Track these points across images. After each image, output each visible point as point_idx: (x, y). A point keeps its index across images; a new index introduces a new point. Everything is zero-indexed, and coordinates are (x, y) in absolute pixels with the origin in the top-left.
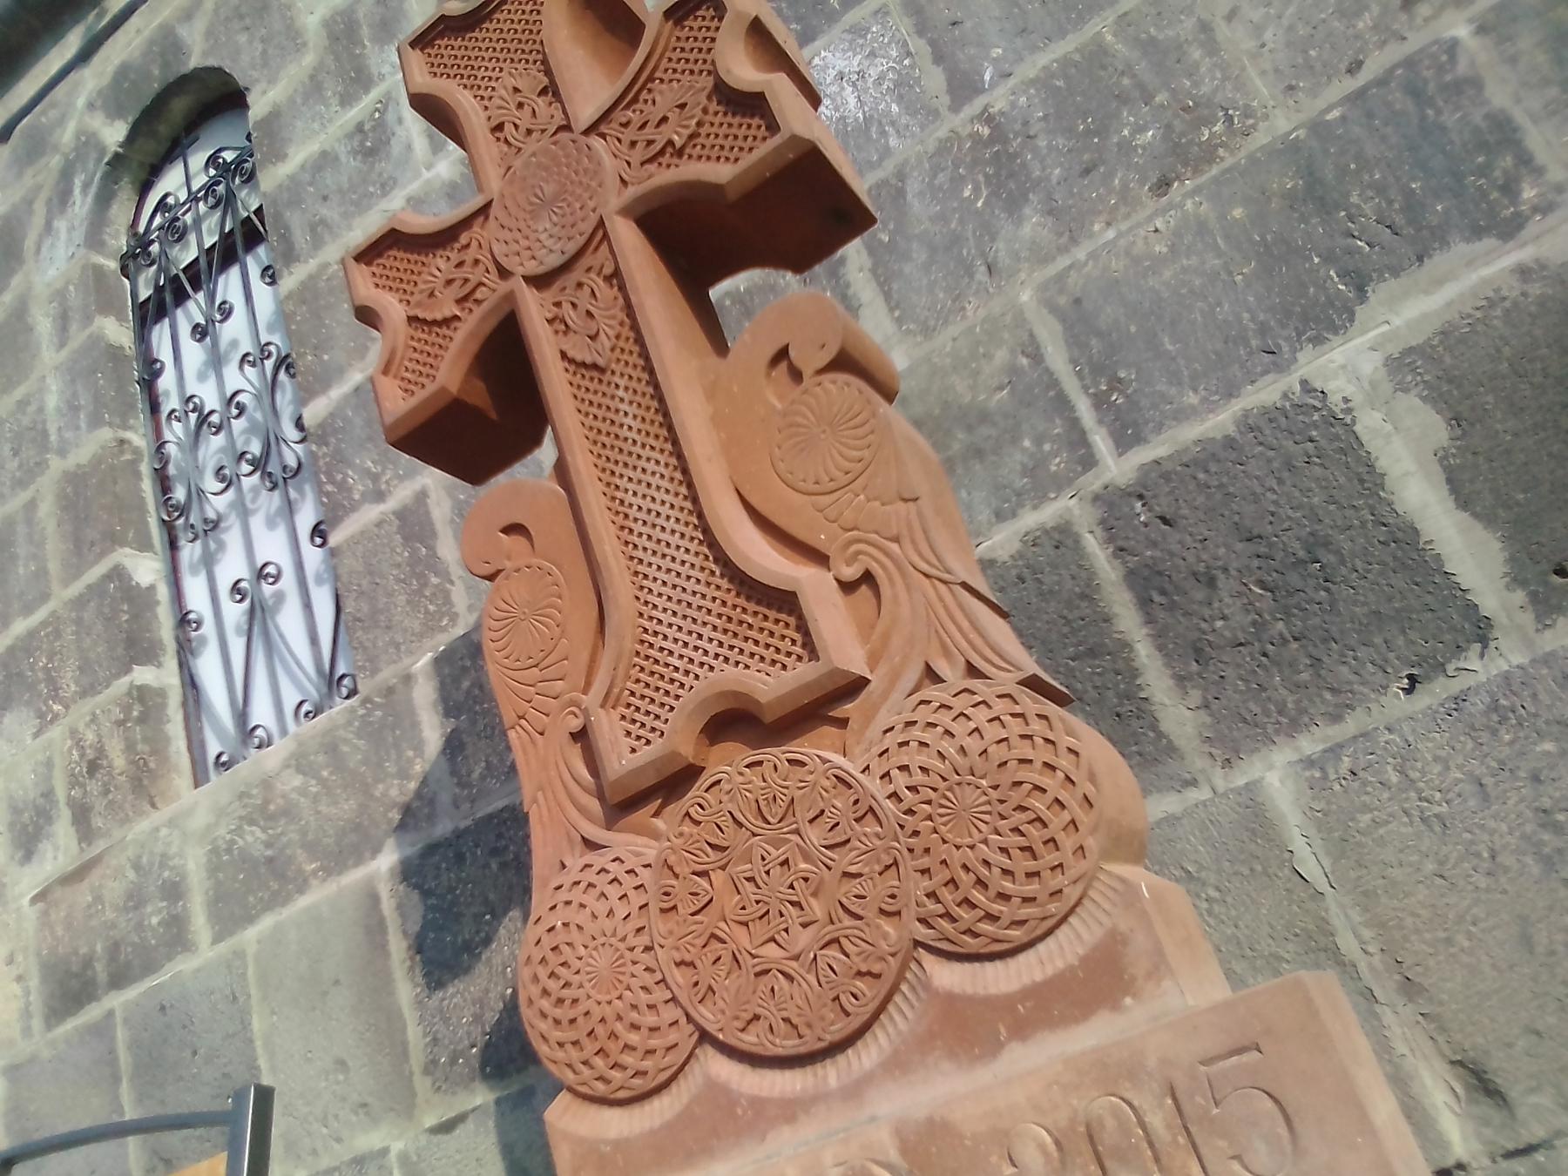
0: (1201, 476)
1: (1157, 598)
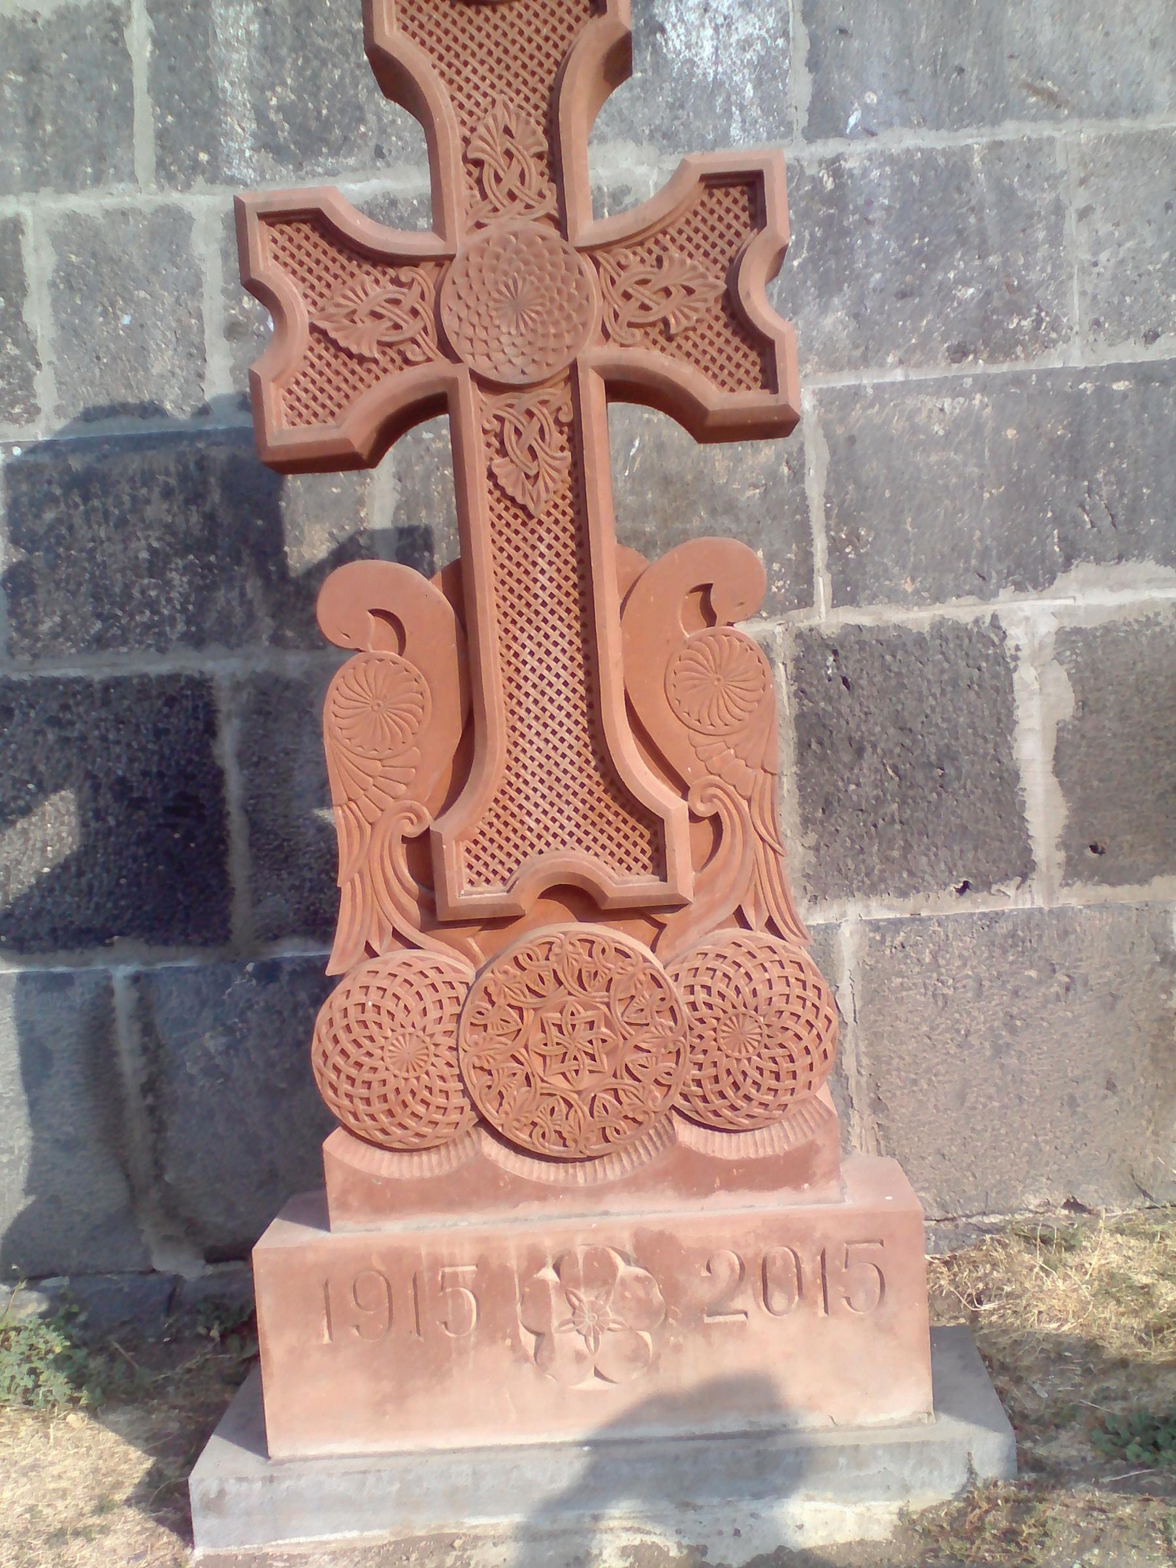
0: (888, 658)
1: (814, 746)
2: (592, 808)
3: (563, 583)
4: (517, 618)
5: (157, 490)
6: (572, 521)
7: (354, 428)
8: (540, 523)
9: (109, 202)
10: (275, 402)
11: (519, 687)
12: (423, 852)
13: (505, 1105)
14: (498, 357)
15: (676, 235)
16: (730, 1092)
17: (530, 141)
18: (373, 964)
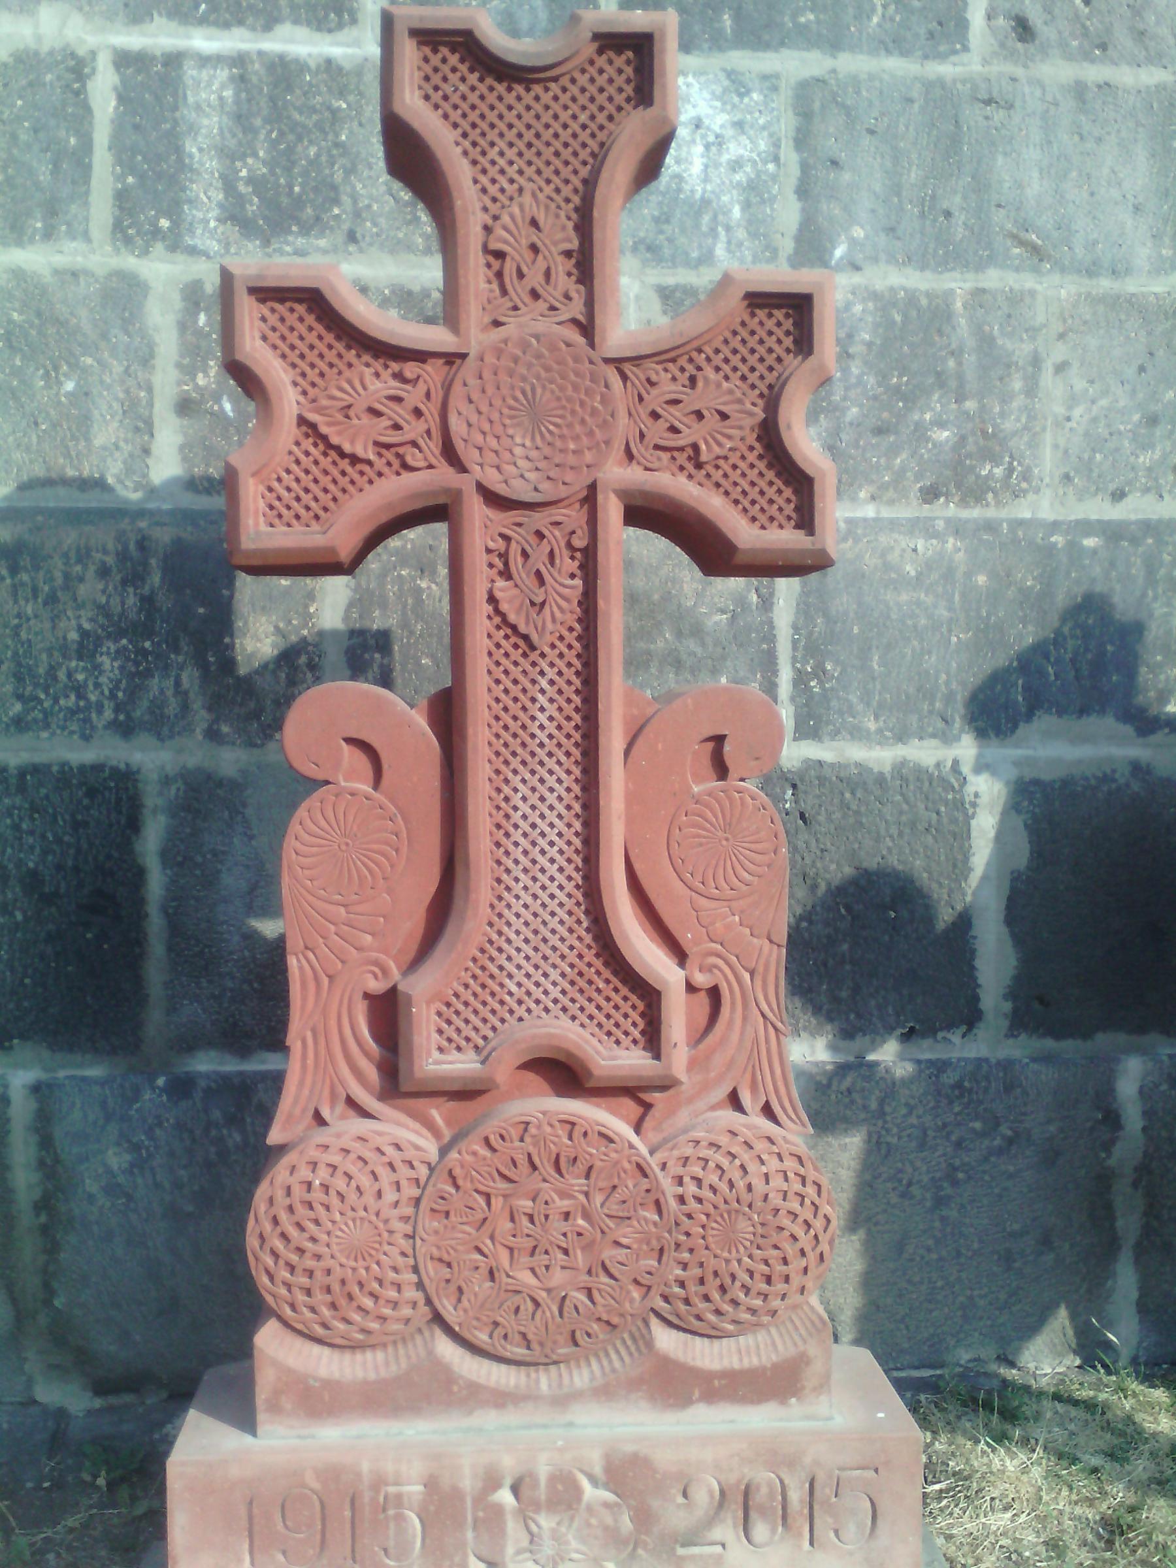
0: (848, 795)
2: (581, 974)
3: (564, 723)
4: (510, 758)
5: (92, 569)
6: (579, 656)
7: (340, 533)
8: (543, 655)
9: (60, 260)
10: (252, 496)
11: (507, 835)
12: (388, 1014)
13: (464, 1299)
14: (510, 469)
15: (712, 355)
16: (716, 1296)
17: (559, 236)
18: (322, 1136)
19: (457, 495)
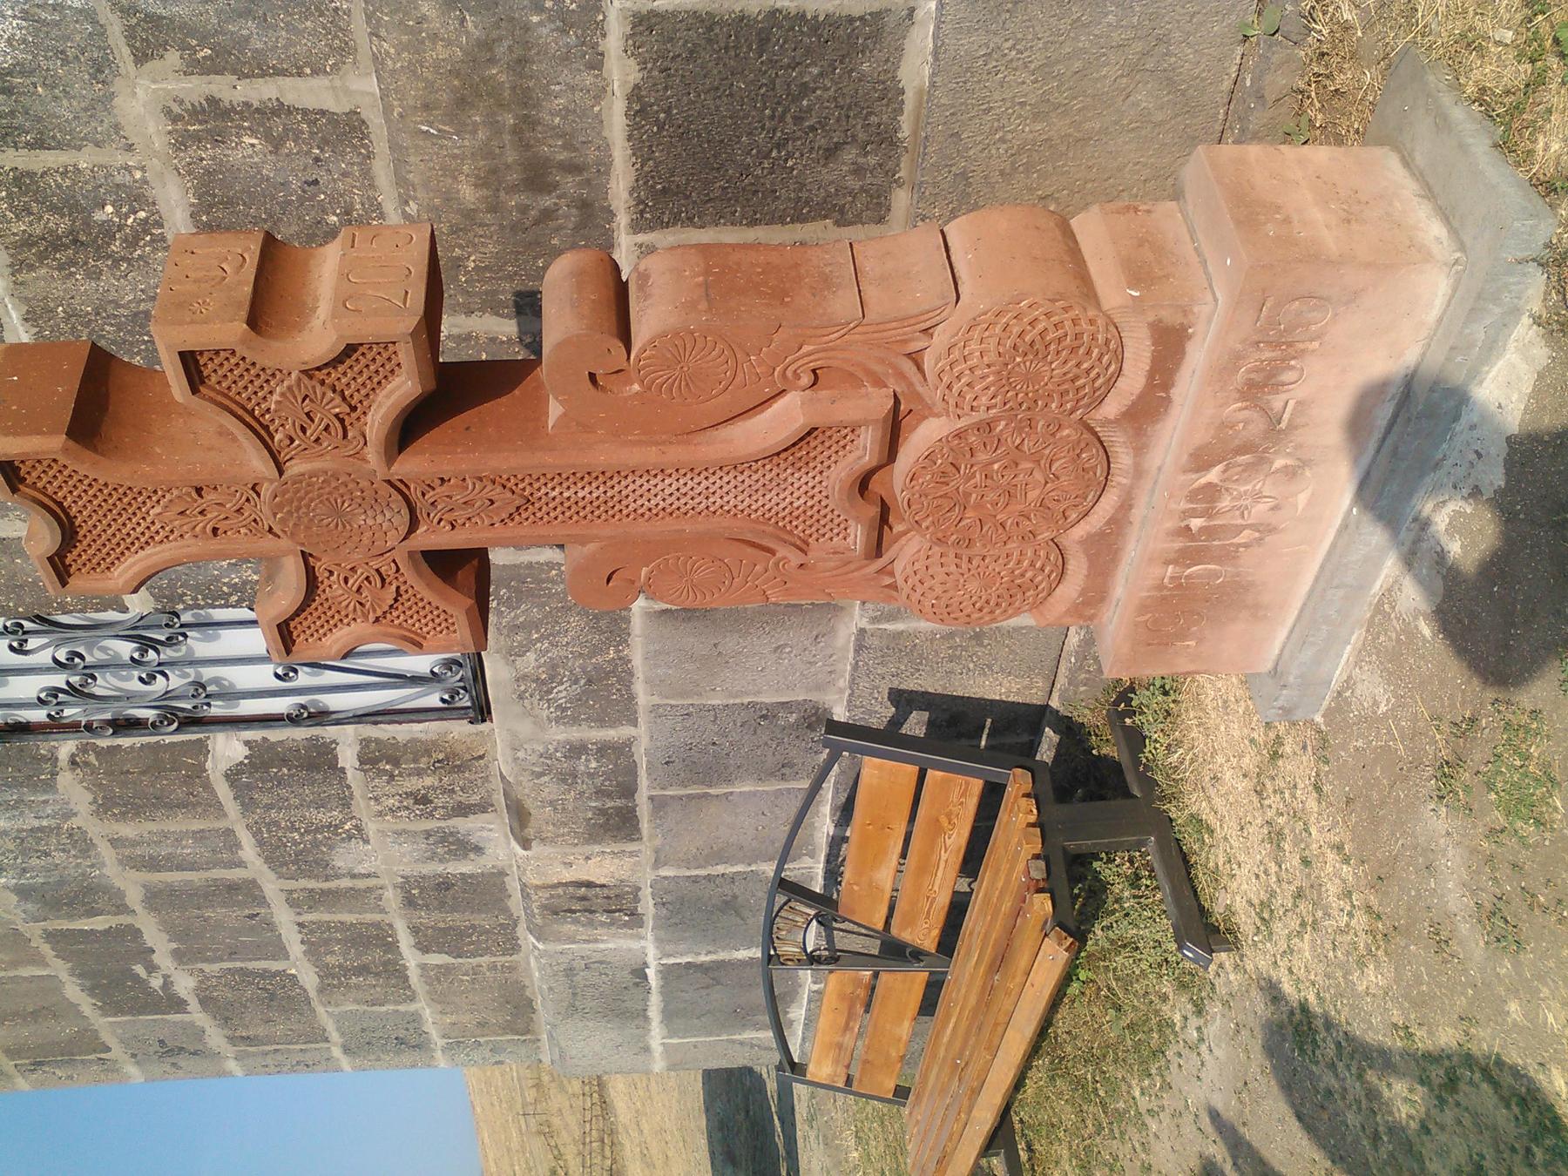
19: (411, 554)
